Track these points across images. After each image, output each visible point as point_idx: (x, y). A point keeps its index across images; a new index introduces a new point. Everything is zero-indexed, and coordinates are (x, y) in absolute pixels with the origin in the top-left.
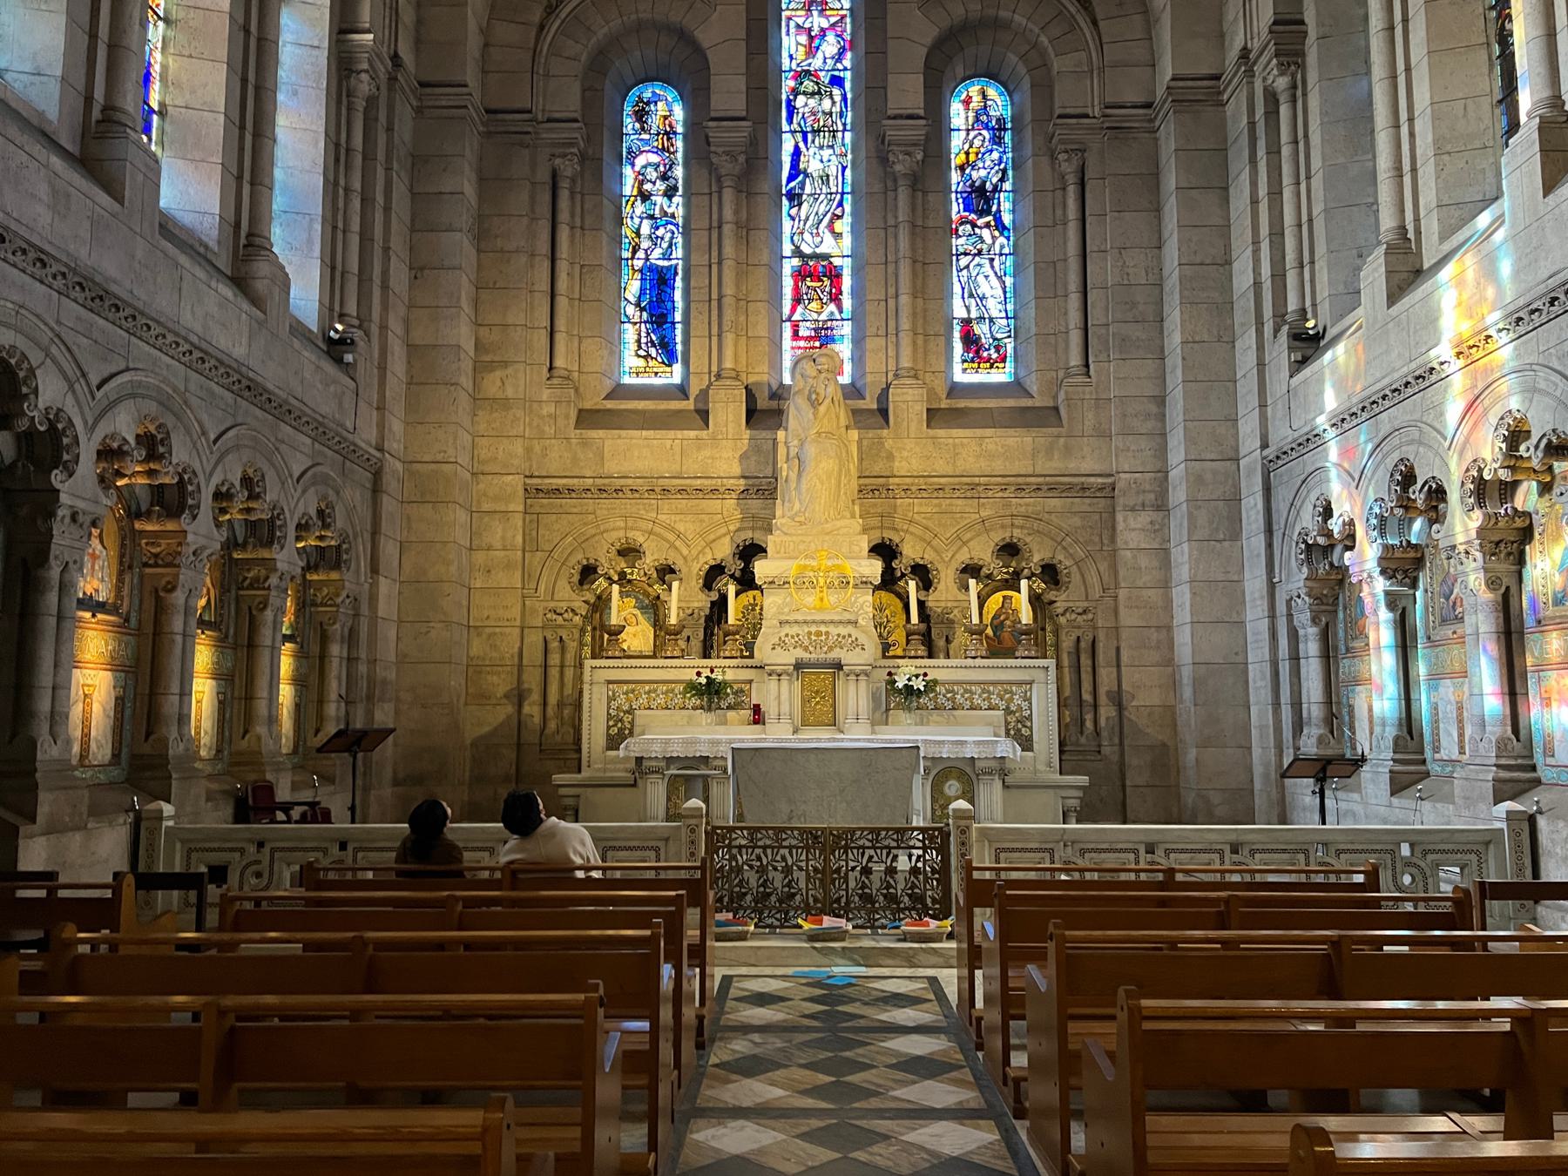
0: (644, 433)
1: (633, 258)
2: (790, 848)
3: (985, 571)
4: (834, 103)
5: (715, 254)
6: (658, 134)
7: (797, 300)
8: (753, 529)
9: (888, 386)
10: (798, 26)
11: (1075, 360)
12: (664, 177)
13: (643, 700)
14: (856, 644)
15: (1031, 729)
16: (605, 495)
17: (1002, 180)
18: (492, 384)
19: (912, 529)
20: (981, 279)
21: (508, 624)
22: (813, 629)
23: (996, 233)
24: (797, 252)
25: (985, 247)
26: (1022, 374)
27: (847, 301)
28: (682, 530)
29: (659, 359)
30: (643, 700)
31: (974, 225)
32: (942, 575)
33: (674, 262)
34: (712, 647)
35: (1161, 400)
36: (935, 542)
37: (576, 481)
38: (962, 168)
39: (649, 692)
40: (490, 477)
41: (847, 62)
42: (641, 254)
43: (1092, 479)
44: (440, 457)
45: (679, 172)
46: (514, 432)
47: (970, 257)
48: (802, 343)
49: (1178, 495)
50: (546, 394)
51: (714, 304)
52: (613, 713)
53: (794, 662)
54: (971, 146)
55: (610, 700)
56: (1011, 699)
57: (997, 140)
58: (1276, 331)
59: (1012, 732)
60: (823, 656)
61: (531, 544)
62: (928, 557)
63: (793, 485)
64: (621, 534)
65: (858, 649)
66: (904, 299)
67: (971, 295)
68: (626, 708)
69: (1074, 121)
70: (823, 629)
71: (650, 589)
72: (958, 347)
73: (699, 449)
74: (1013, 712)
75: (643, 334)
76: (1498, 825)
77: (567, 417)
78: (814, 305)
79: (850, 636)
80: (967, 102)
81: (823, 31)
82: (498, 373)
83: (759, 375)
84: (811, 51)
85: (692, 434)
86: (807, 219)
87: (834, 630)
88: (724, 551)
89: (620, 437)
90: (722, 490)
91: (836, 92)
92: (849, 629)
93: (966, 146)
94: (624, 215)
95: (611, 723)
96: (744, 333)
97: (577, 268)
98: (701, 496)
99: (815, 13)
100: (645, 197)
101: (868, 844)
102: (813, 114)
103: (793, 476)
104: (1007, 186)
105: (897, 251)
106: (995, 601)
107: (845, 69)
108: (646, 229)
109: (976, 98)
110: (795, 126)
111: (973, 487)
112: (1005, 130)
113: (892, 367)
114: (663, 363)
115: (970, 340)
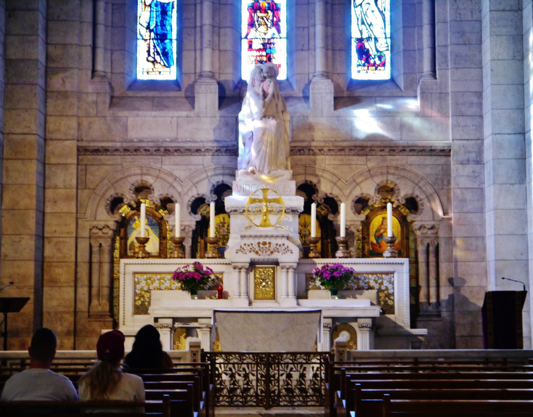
0: (154, 113)
2: (248, 364)
3: (370, 203)
7: (252, 24)
8: (223, 174)
9: (310, 82)
13: (156, 284)
14: (287, 250)
15: (393, 300)
16: (129, 153)
18: (56, 83)
20: (369, 13)
21: (67, 235)
26: (395, 74)
27: (283, 25)
30: (156, 284)
34: (197, 251)
35: (480, 94)
36: (339, 184)
39: (159, 279)
40: (55, 142)
44: (26, 131)
46: (70, 113)
49: (488, 155)
50: (90, 88)
52: (138, 292)
53: (249, 261)
55: (135, 284)
56: (382, 283)
59: (382, 303)
62: (335, 192)
64: (138, 178)
65: (289, 253)
66: (319, 29)
67: (363, 23)
68: (146, 288)
71: (156, 213)
74: (383, 291)
75: (152, 47)
77: (104, 103)
78: (262, 29)
79: (284, 245)
82: (61, 75)
83: (228, 77)
85: (184, 113)
87: (274, 241)
89: (138, 116)
90: (203, 150)
92: (285, 241)
95: (137, 298)
96: (217, 48)
97: (110, 6)
98: (189, 153)
101: (290, 361)
114: (165, 65)
115: (363, 53)
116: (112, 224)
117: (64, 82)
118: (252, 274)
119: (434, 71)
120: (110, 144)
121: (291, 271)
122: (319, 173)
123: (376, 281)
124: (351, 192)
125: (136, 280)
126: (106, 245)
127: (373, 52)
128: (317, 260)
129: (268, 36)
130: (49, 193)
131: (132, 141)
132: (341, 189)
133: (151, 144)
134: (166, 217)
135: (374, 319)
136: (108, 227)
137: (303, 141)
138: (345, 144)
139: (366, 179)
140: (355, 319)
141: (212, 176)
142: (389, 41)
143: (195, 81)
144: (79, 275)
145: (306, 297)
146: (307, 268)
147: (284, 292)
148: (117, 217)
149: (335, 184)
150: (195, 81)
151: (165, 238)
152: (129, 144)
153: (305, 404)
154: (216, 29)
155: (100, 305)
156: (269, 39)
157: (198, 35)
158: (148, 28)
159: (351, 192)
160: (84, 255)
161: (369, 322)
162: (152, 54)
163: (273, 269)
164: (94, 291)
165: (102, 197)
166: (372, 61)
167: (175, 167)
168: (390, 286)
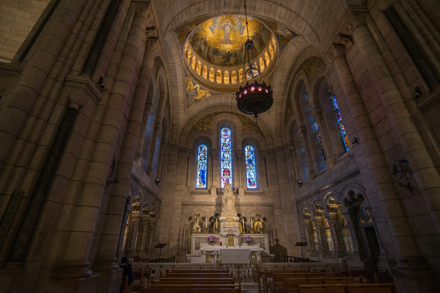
7: (224, 175)
8: (218, 211)
10: (223, 138)
12: (204, 157)
13: (201, 241)
14: (237, 231)
17: (253, 159)
18: (178, 188)
20: (251, 173)
22: (230, 229)
24: (223, 168)
27: (231, 176)
31: (249, 165)
37: (190, 203)
38: (247, 157)
39: (202, 240)
41: (230, 142)
42: (200, 168)
43: (270, 204)
45: (206, 157)
48: (224, 182)
51: (212, 176)
52: (196, 243)
55: (196, 241)
56: (261, 241)
57: (252, 153)
58: (295, 183)
61: (182, 213)
63: (225, 204)
67: (249, 175)
68: (198, 242)
70: (231, 229)
72: (248, 183)
78: (226, 176)
80: (247, 148)
81: (227, 138)
82: (179, 186)
85: (208, 196)
87: (233, 229)
88: (213, 215)
91: (229, 146)
100: (201, 160)
103: (225, 203)
104: (254, 160)
108: (201, 164)
109: (249, 148)
110: (223, 151)
111: (252, 205)
113: (239, 185)
115: (250, 182)
119: (268, 186)
123: (260, 241)
127: (252, 182)
128: (244, 234)
134: (203, 222)
135: (261, 252)
138: (247, 204)
140: (256, 252)
143: (211, 188)
145: (241, 245)
146: (242, 237)
149: (246, 214)
150: (211, 188)
151: (202, 228)
153: (250, 281)
158: (199, 175)
160: (181, 233)
161: (260, 252)
163: (233, 237)
168: (263, 242)
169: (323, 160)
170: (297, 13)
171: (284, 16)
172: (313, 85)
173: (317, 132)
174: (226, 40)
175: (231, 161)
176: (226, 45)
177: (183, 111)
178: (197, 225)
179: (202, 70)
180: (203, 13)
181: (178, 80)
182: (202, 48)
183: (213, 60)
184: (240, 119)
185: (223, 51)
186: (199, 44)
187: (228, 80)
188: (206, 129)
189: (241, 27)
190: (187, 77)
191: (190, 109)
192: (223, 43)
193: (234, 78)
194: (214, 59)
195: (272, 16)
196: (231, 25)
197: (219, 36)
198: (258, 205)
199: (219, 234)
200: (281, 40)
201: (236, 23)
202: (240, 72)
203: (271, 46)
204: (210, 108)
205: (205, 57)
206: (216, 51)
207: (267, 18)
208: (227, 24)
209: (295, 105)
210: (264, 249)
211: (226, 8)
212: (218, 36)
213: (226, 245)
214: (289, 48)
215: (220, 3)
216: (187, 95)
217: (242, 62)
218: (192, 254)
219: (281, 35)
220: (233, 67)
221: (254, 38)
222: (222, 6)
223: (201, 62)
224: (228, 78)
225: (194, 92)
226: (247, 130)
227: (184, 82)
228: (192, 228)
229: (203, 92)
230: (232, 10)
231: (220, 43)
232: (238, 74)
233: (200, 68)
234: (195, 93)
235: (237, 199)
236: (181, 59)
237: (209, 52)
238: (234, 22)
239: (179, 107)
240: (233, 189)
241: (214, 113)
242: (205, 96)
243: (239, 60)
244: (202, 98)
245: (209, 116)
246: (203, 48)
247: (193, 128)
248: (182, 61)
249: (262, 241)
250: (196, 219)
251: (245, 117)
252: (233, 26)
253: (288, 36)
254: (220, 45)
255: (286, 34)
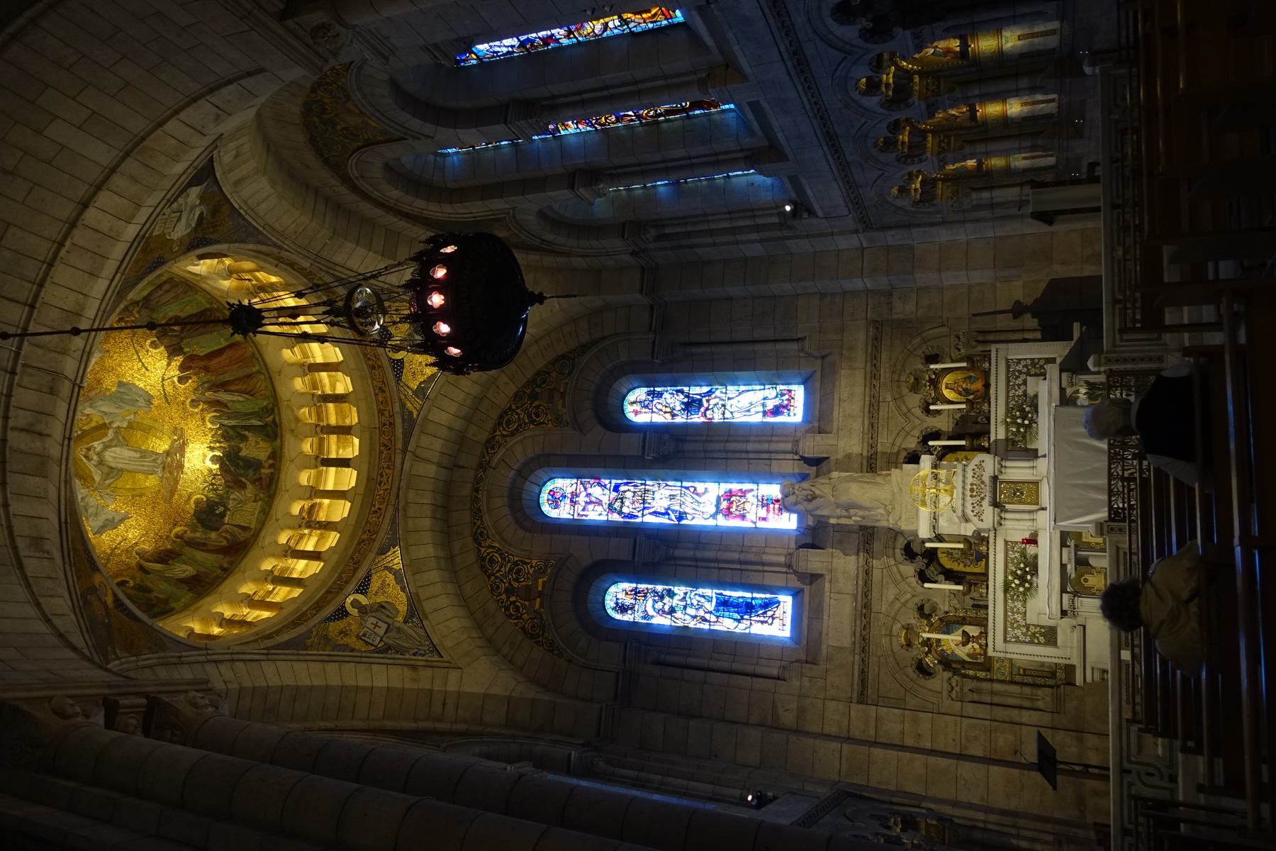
0: (825, 617)
1: (709, 622)
4: (629, 490)
5: (712, 565)
6: (636, 599)
7: (743, 517)
8: (894, 548)
10: (584, 510)
11: (794, 346)
12: (662, 597)
13: (1019, 617)
14: (980, 466)
15: (1040, 359)
16: (867, 648)
17: (682, 392)
18: (788, 718)
19: (898, 444)
20: (739, 405)
23: (713, 396)
25: (721, 402)
28: (893, 597)
29: (775, 609)
30: (1019, 617)
31: (707, 409)
32: (931, 425)
33: (714, 595)
36: (907, 429)
38: (673, 416)
39: (1012, 612)
40: (851, 726)
41: (607, 482)
42: (707, 616)
44: (837, 755)
45: (659, 588)
47: (726, 411)
51: (744, 567)
52: (1028, 639)
53: (992, 508)
54: (661, 410)
55: (1018, 641)
56: (1020, 372)
58: (790, 228)
60: (987, 487)
61: (899, 704)
63: (867, 513)
65: (983, 464)
67: (749, 411)
68: (1024, 630)
69: (656, 349)
73: (837, 581)
74: (1028, 370)
75: (758, 619)
76: (1097, 71)
78: (747, 506)
79: (974, 470)
80: (636, 413)
81: (588, 495)
84: (599, 503)
85: (827, 585)
86: (694, 509)
87: (970, 480)
88: (909, 569)
89: (827, 635)
90: (866, 567)
91: (622, 488)
93: (661, 413)
94: (682, 625)
95: (1036, 641)
99: (577, 499)
100: (672, 611)
102: (633, 503)
103: (861, 513)
105: (720, 451)
106: (948, 394)
107: (610, 483)
108: (691, 611)
110: (640, 514)
111: (871, 405)
112: (654, 390)
113: (790, 456)
114: (777, 607)
115: (777, 411)
116: (947, 675)
117: (787, 710)
118: (1008, 507)
119: (798, 340)
120: (856, 667)
121: (1003, 464)
122: (896, 449)
123: (1018, 377)
124: (917, 417)
125: (1013, 640)
126: (970, 684)
127: (777, 402)
129: (755, 501)
130: (909, 742)
131: (854, 643)
132: (914, 428)
133: (858, 622)
135: (1061, 371)
136: (949, 679)
137: (862, 464)
138: (866, 423)
139: (904, 402)
140: (1062, 390)
141: (895, 560)
142: (767, 387)
144: (1007, 719)
146: (1001, 448)
147: (1030, 471)
148: (940, 668)
149: (908, 433)
150: (795, 572)
151: (964, 618)
152: (857, 646)
154: (744, 550)
155: (1043, 699)
156: (758, 500)
157: (749, 567)
158: (739, 621)
159: (917, 417)
160: (983, 711)
161: (1064, 375)
162: (766, 619)
163: (1001, 483)
164: (1026, 703)
165: (915, 682)
166: (786, 402)
167: (884, 599)
168: (1023, 363)
169: (710, 114)
170: (131, 144)
171: (125, 201)
172: (415, 123)
173: (599, 128)
174: (164, 468)
175: (685, 484)
176: (185, 470)
177: (454, 675)
178: (951, 641)
179: (283, 580)
180: (50, 529)
181: (317, 682)
182: (184, 575)
183: (245, 529)
184: (513, 434)
185: (213, 484)
186: (163, 586)
187: (336, 473)
188: (540, 581)
189: (121, 400)
190: (309, 642)
191: (448, 643)
192: (177, 482)
193: (333, 447)
194: (238, 526)
195: (119, 250)
196: (105, 440)
197: (141, 496)
198: (874, 381)
199: (991, 541)
200: (214, 231)
201: (96, 420)
202: (310, 421)
203: (225, 279)
204: (451, 558)
205: (226, 565)
206: (204, 516)
207: (117, 272)
208: (95, 458)
209: (480, 202)
210: (1052, 361)
211: (46, 432)
212: (144, 499)
213: (1037, 511)
214: (250, 202)
215: (22, 452)
216: (387, 649)
217: (270, 406)
218: (1076, 660)
219: (194, 225)
220: (286, 450)
221: (175, 350)
222: (38, 444)
223: (244, 581)
224: (332, 470)
225: (375, 621)
226: (560, 407)
227: (326, 658)
228: (964, 662)
229: (380, 582)
230: (61, 409)
231: (172, 495)
232: (319, 430)
233: (270, 587)
234: (378, 614)
235: (845, 464)
236: (228, 657)
237: (205, 544)
238: (93, 424)
239: (431, 691)
240: (804, 477)
241: (476, 540)
242: (396, 573)
243: (261, 419)
244: (403, 589)
245: (485, 564)
246: (183, 570)
247: (532, 637)
248: (236, 657)
249: (1020, 367)
250: (927, 642)
251: (505, 412)
252: (111, 433)
253: (203, 198)
254: (180, 495)
255: (193, 208)
